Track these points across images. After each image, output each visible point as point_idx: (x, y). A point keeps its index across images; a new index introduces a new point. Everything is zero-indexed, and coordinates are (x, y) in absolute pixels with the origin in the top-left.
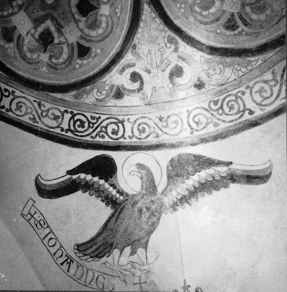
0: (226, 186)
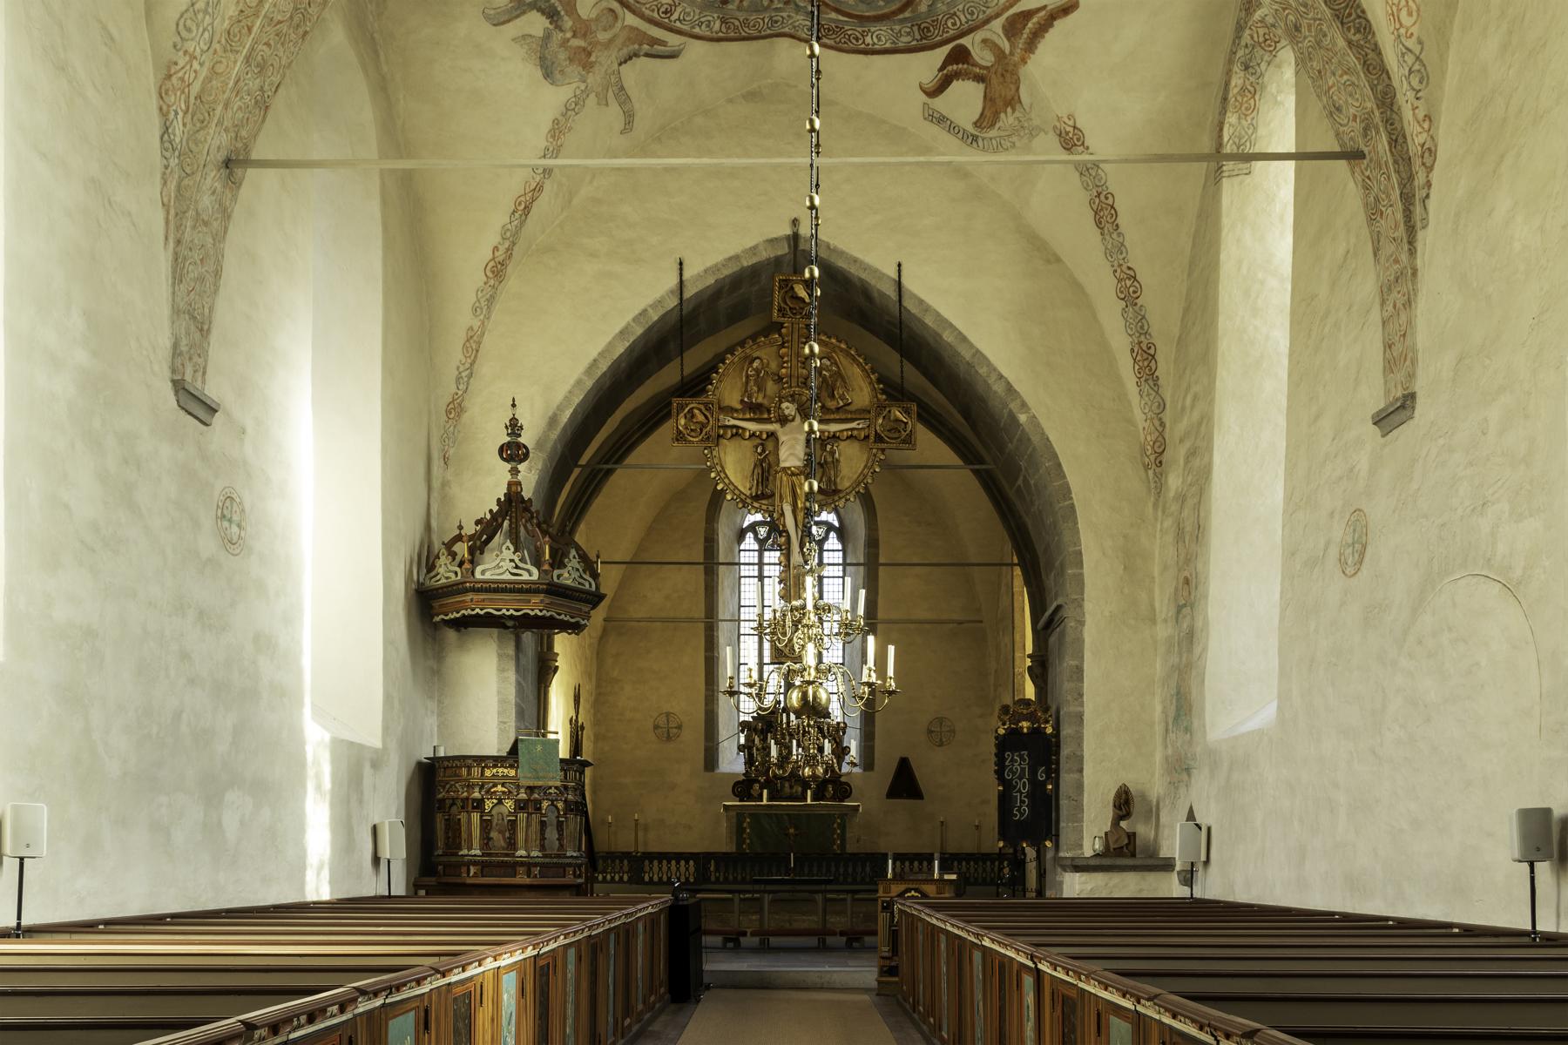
0: (1051, 25)
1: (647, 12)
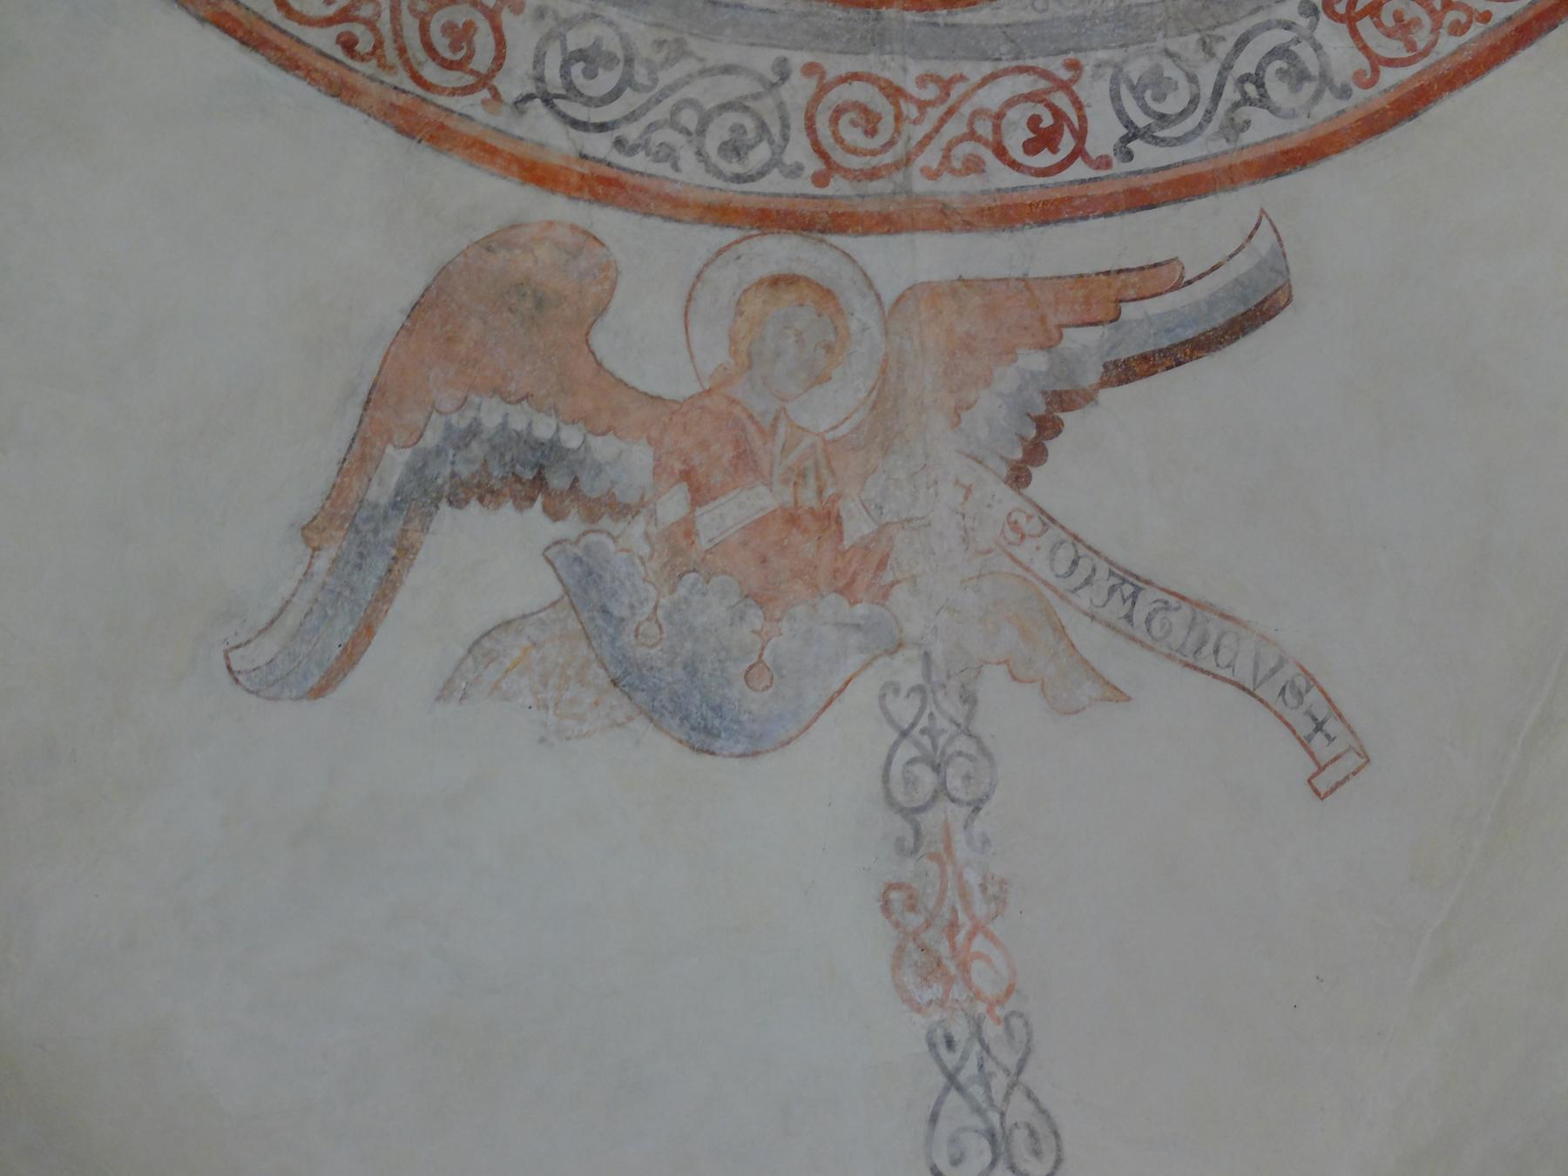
1: (952, 188)
